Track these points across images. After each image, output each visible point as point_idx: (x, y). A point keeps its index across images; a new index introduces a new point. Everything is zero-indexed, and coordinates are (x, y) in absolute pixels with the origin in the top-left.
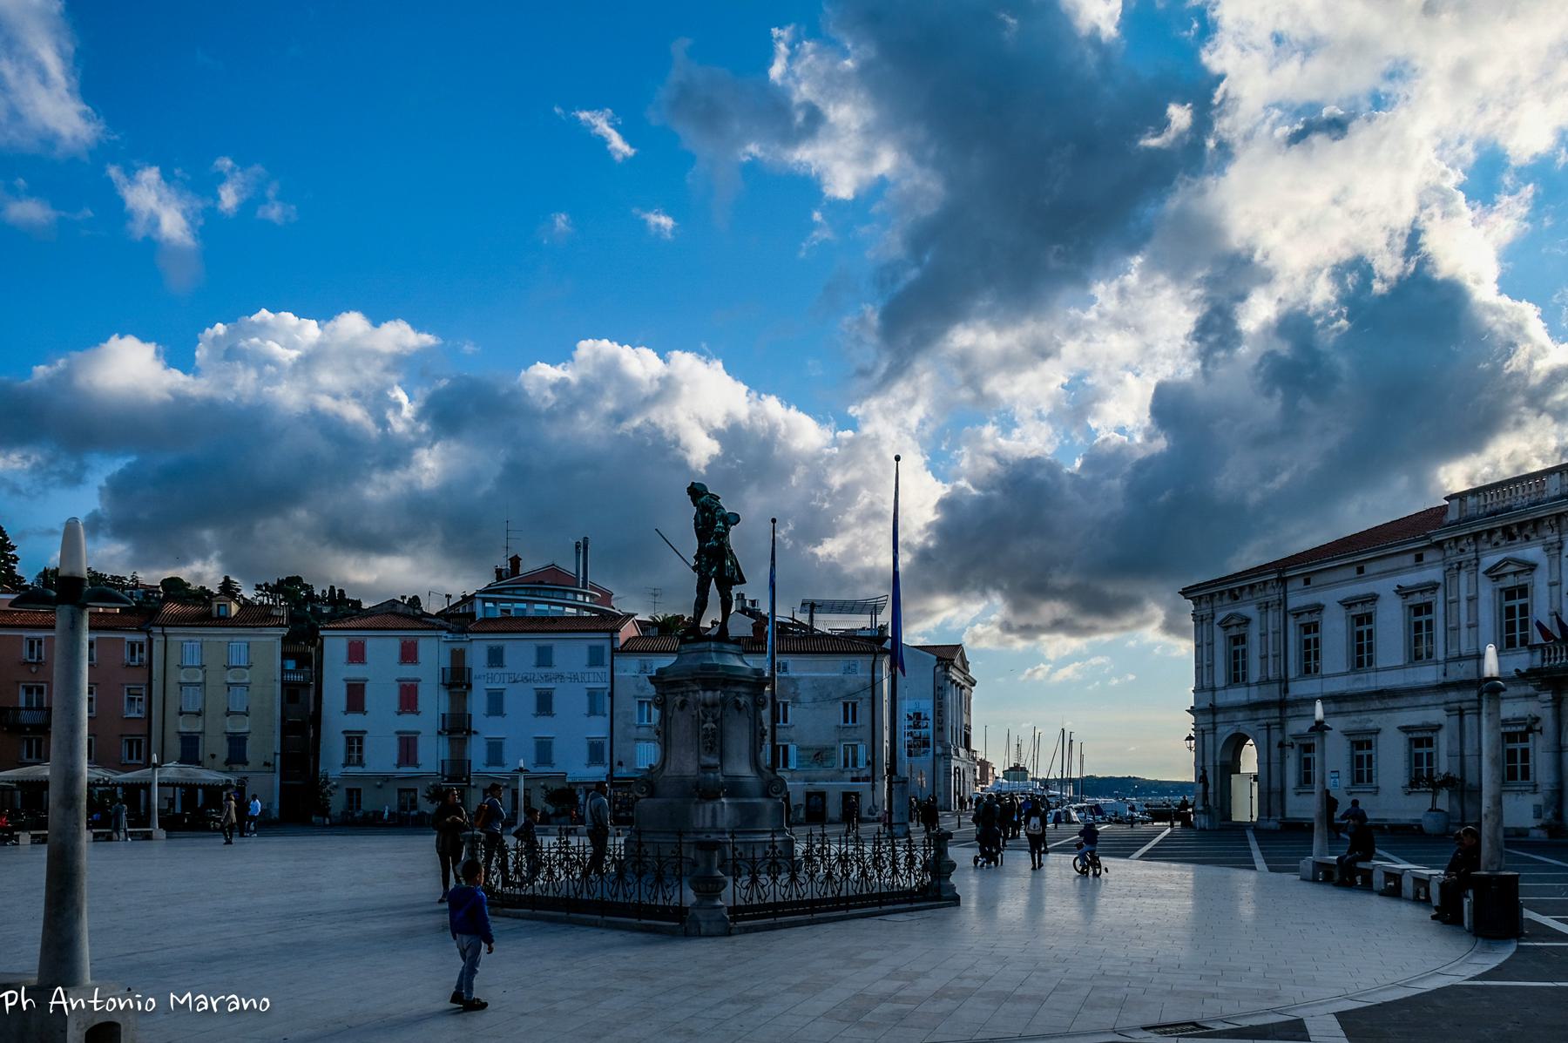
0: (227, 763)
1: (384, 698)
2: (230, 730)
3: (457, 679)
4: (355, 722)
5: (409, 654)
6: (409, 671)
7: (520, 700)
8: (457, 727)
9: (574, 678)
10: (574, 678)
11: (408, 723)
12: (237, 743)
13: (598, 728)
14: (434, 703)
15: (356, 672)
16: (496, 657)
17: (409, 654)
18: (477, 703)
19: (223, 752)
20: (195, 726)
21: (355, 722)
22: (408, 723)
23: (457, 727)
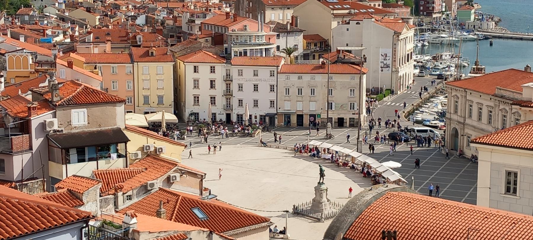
0: (158, 104)
1: (204, 84)
3: (228, 79)
4: (196, 92)
5: (213, 70)
6: (213, 76)
7: (248, 87)
8: (228, 94)
9: (265, 80)
10: (265, 80)
11: (213, 92)
12: (160, 99)
13: (272, 96)
14: (220, 86)
16: (240, 73)
17: (213, 70)
18: (234, 87)
20: (147, 93)
22: (213, 92)
23: (228, 94)
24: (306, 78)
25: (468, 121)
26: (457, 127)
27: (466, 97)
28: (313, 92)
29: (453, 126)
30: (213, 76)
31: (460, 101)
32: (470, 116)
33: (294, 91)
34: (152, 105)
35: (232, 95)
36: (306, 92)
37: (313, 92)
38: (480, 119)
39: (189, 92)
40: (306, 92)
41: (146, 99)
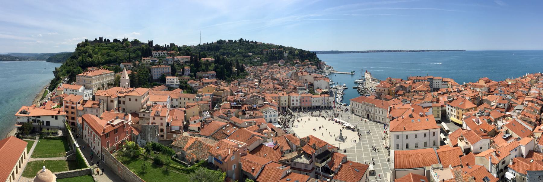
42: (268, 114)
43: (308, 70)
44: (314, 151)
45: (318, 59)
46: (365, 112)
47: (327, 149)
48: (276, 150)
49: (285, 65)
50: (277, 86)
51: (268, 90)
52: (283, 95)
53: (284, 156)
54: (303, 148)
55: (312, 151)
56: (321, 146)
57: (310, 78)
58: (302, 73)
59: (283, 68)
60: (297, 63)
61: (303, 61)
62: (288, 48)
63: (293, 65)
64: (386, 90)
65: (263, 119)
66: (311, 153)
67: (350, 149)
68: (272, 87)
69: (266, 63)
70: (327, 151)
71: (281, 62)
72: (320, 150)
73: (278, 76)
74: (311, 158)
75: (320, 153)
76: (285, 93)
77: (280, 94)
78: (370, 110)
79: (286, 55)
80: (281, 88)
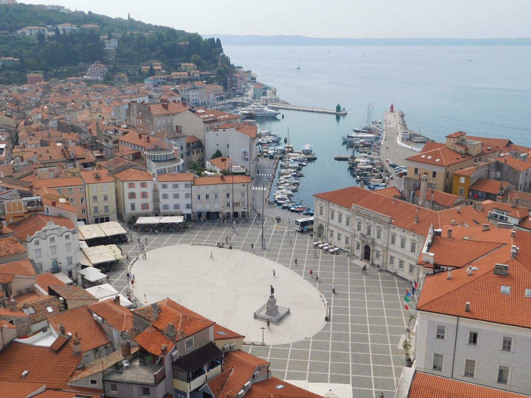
2: (105, 205)
3: (156, 191)
6: (144, 189)
11: (145, 201)
13: (189, 201)
15: (132, 190)
19: (103, 210)
21: (132, 201)
24: (212, 187)
25: (331, 221)
26: (323, 224)
27: (329, 206)
28: (216, 196)
29: (319, 223)
30: (144, 189)
31: (324, 209)
32: (332, 218)
33: (203, 197)
34: (100, 213)
35: (159, 201)
36: (212, 196)
37: (216, 196)
38: (340, 220)
39: (128, 202)
40: (212, 196)
41: (96, 209)
42: (45, 245)
43: (193, 96)
44: (171, 346)
45: (226, 60)
46: (357, 240)
47: (212, 339)
48: (58, 351)
49: (108, 79)
50: (75, 150)
51: (45, 165)
52: (98, 178)
53: (83, 369)
54: (140, 340)
55: (164, 346)
56: (190, 330)
57: (191, 124)
58: (166, 107)
59: (101, 91)
60: (152, 72)
61: (176, 68)
62: (119, 21)
63: (137, 78)
64: (441, 172)
65: (23, 264)
66: (158, 353)
67: (295, 345)
68: (57, 156)
69: (40, 75)
70: (211, 346)
71: (95, 71)
72: (189, 343)
73: (81, 117)
74: (161, 363)
75: (188, 350)
76: (103, 173)
77: (88, 174)
78: (374, 234)
79: (111, 45)
80: (91, 155)
